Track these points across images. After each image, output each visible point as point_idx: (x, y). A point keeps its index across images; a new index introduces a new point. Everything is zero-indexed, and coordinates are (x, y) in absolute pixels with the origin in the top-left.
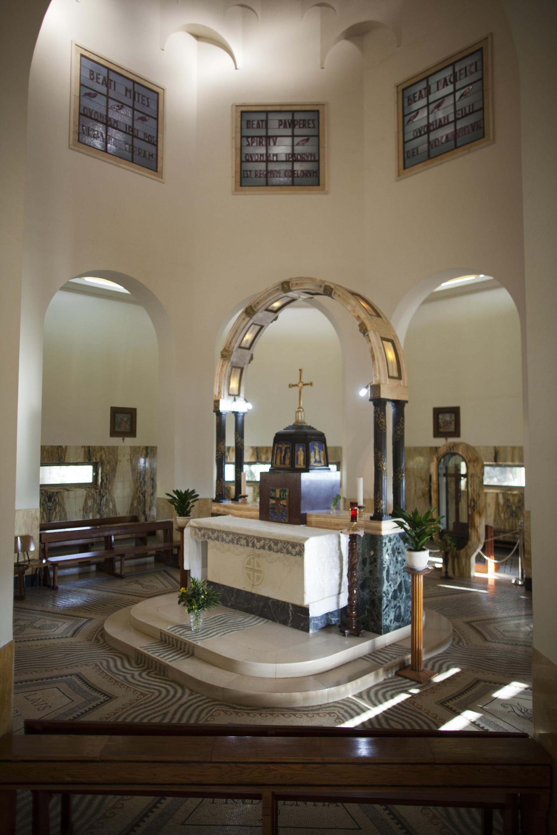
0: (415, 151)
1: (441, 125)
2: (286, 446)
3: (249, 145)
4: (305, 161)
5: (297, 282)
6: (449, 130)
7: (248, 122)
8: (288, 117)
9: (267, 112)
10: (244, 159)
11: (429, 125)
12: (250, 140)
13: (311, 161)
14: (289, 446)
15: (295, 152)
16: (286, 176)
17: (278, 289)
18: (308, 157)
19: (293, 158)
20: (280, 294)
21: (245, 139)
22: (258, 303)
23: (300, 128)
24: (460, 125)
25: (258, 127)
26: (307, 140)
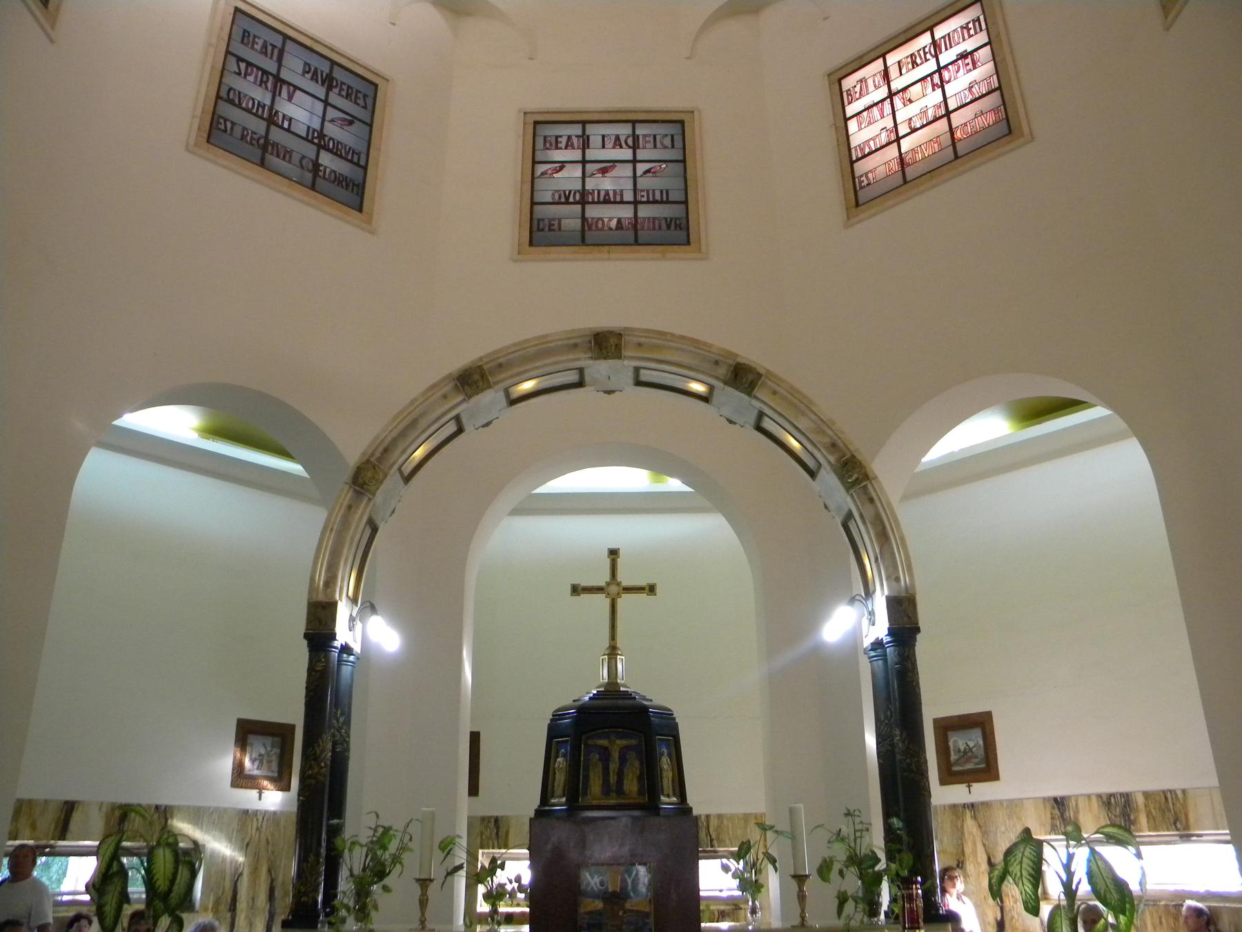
0: (556, 223)
1: (606, 200)
2: (624, 742)
3: (239, 74)
4: (340, 156)
5: (643, 340)
6: (626, 212)
7: (246, 33)
8: (325, 67)
9: (286, 37)
10: (223, 94)
11: (584, 192)
12: (243, 66)
13: (351, 161)
14: (634, 742)
15: (325, 132)
16: (302, 167)
17: (575, 346)
18: (347, 153)
19: (319, 139)
20: (578, 359)
21: (232, 60)
22: (500, 365)
23: (340, 94)
24: (645, 212)
25: (264, 51)
26: (351, 123)
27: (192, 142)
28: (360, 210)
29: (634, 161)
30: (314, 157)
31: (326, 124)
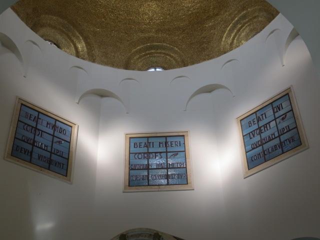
27: (6, 156)
28: (66, 176)
29: (167, 152)
30: (49, 157)
31: (54, 144)
